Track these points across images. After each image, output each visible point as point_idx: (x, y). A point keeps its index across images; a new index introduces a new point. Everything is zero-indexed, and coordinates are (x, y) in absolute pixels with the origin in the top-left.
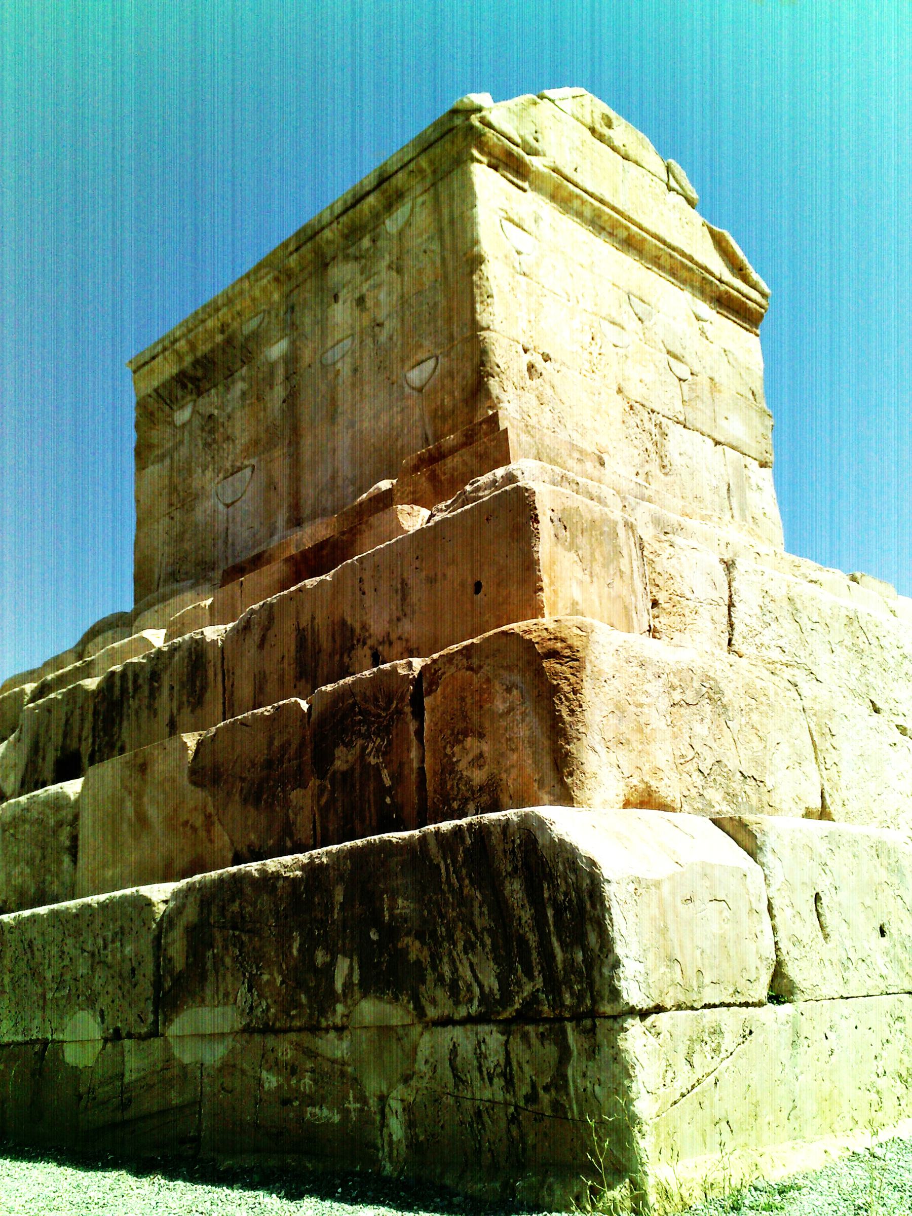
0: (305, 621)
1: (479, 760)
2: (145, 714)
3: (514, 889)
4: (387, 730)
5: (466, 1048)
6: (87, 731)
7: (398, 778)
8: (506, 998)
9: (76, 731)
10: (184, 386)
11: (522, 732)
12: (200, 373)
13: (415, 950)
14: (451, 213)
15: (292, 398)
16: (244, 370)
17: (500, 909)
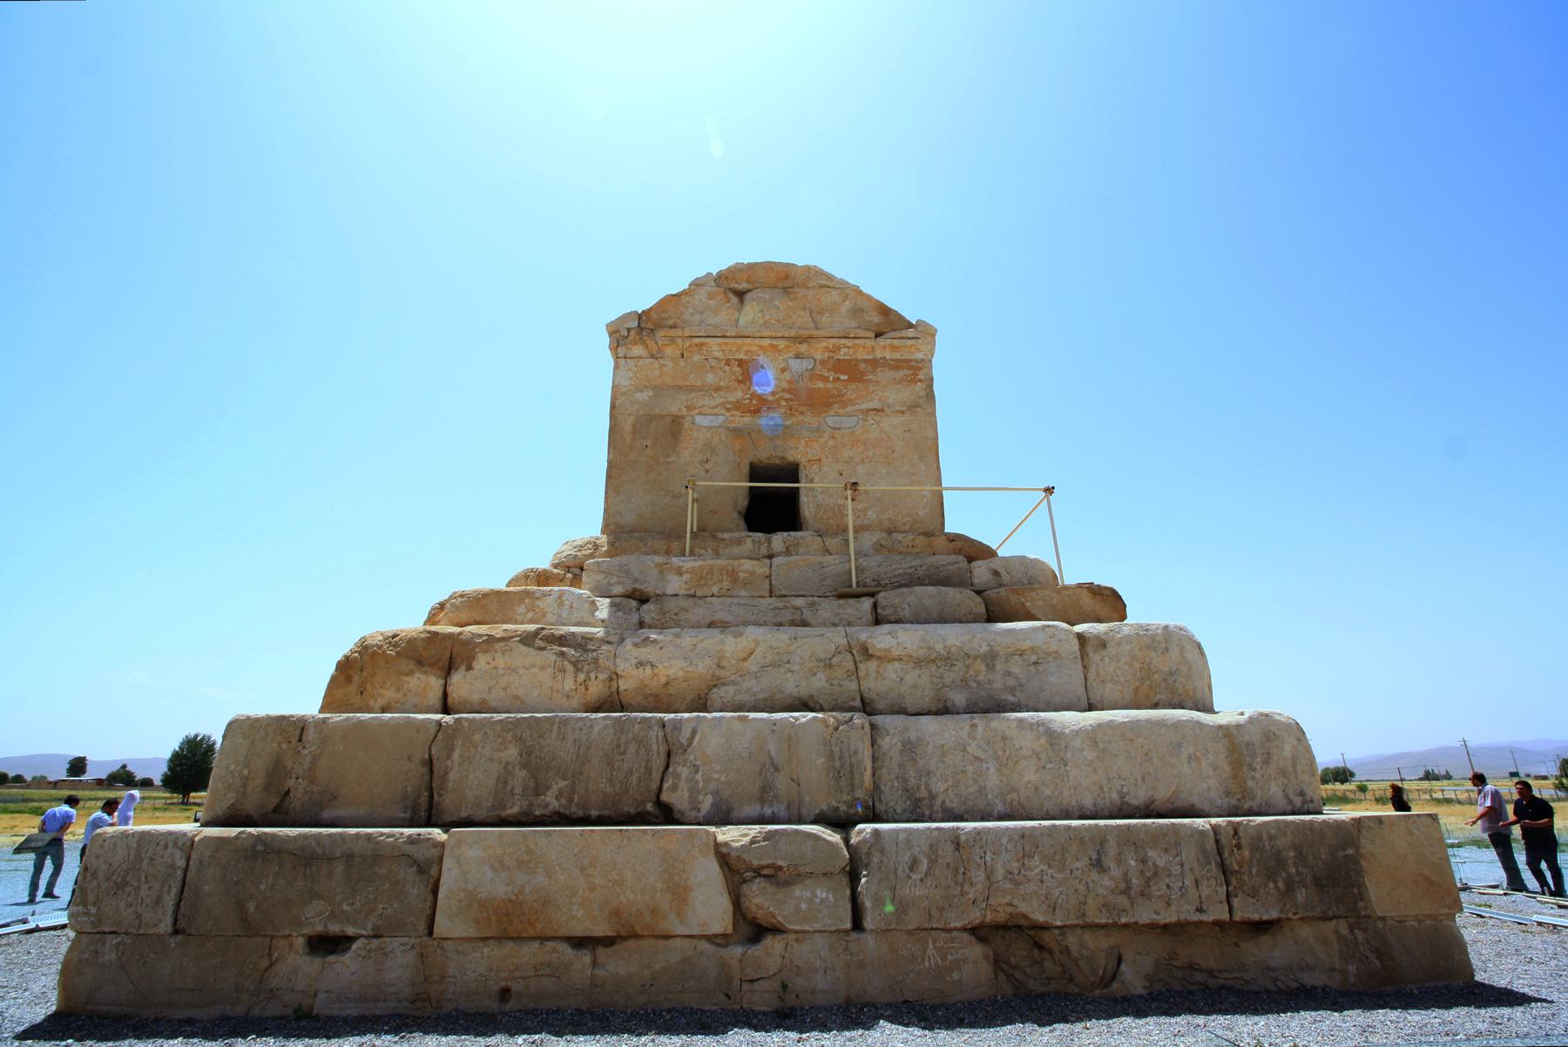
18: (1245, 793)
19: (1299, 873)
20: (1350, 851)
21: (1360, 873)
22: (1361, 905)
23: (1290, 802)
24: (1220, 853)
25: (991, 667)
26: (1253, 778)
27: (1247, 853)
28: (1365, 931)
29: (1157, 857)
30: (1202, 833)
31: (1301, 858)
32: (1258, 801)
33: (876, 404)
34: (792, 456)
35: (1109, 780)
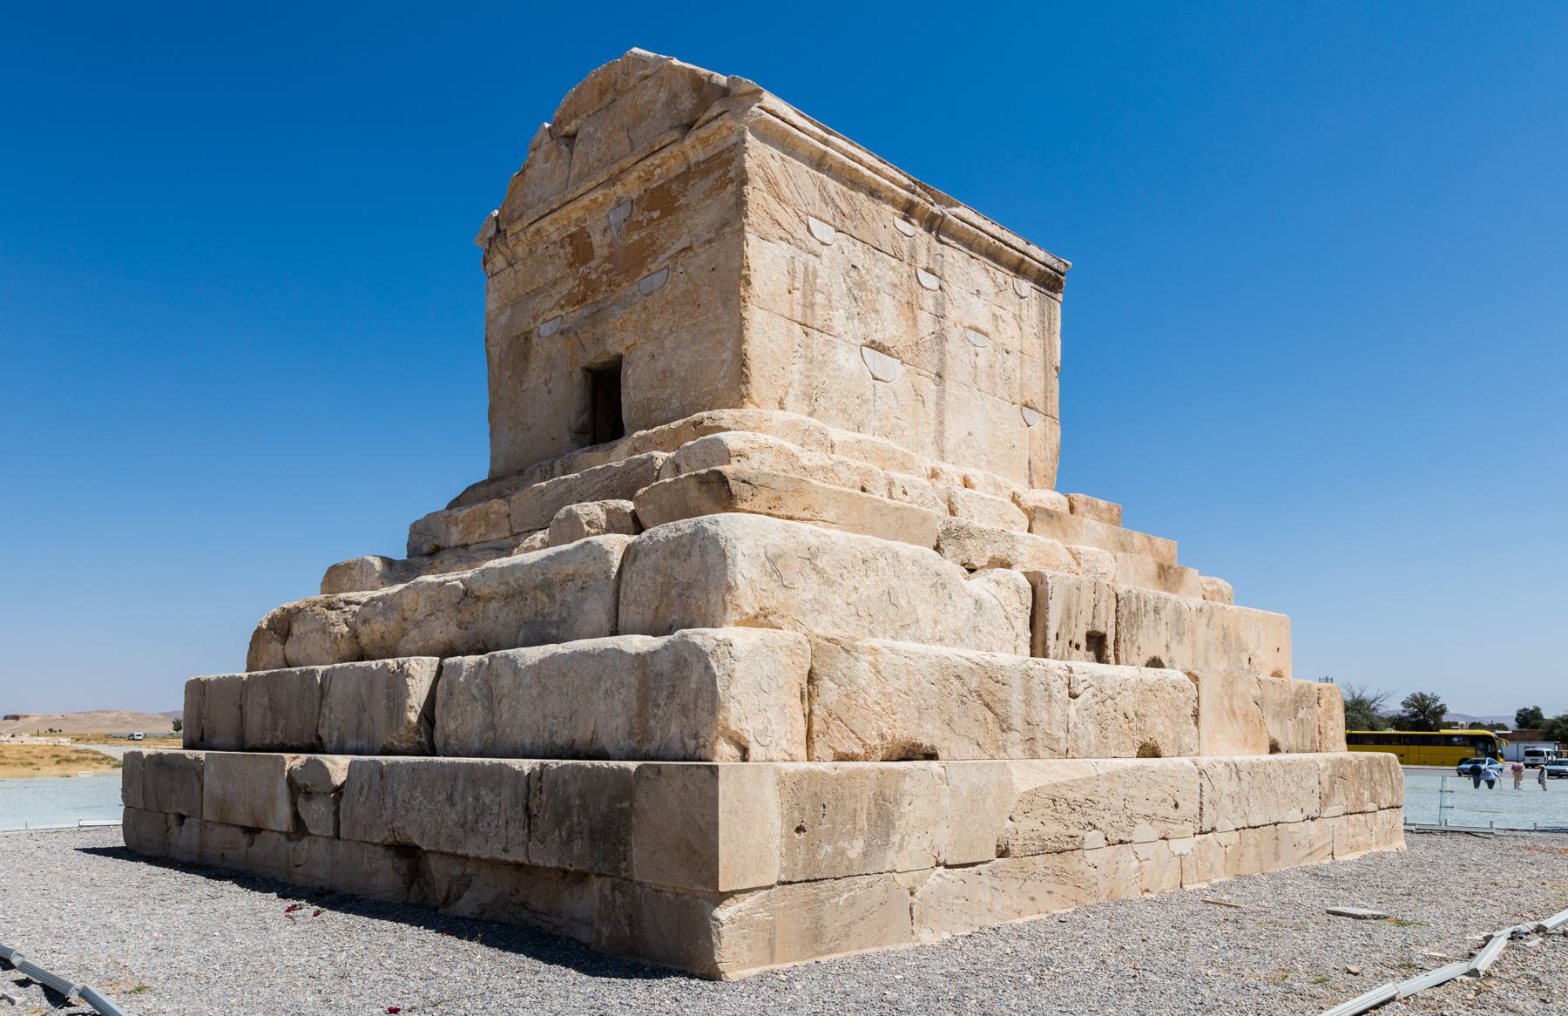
2: (1152, 632)
6: (1112, 621)
18: (646, 734)
19: (580, 823)
20: (626, 804)
21: (629, 830)
22: (623, 865)
23: (684, 745)
24: (527, 797)
25: (552, 597)
26: (655, 716)
27: (544, 797)
28: (624, 893)
29: (487, 797)
30: (519, 774)
31: (584, 807)
32: (655, 744)
33: (684, 243)
34: (614, 347)
35: (545, 718)
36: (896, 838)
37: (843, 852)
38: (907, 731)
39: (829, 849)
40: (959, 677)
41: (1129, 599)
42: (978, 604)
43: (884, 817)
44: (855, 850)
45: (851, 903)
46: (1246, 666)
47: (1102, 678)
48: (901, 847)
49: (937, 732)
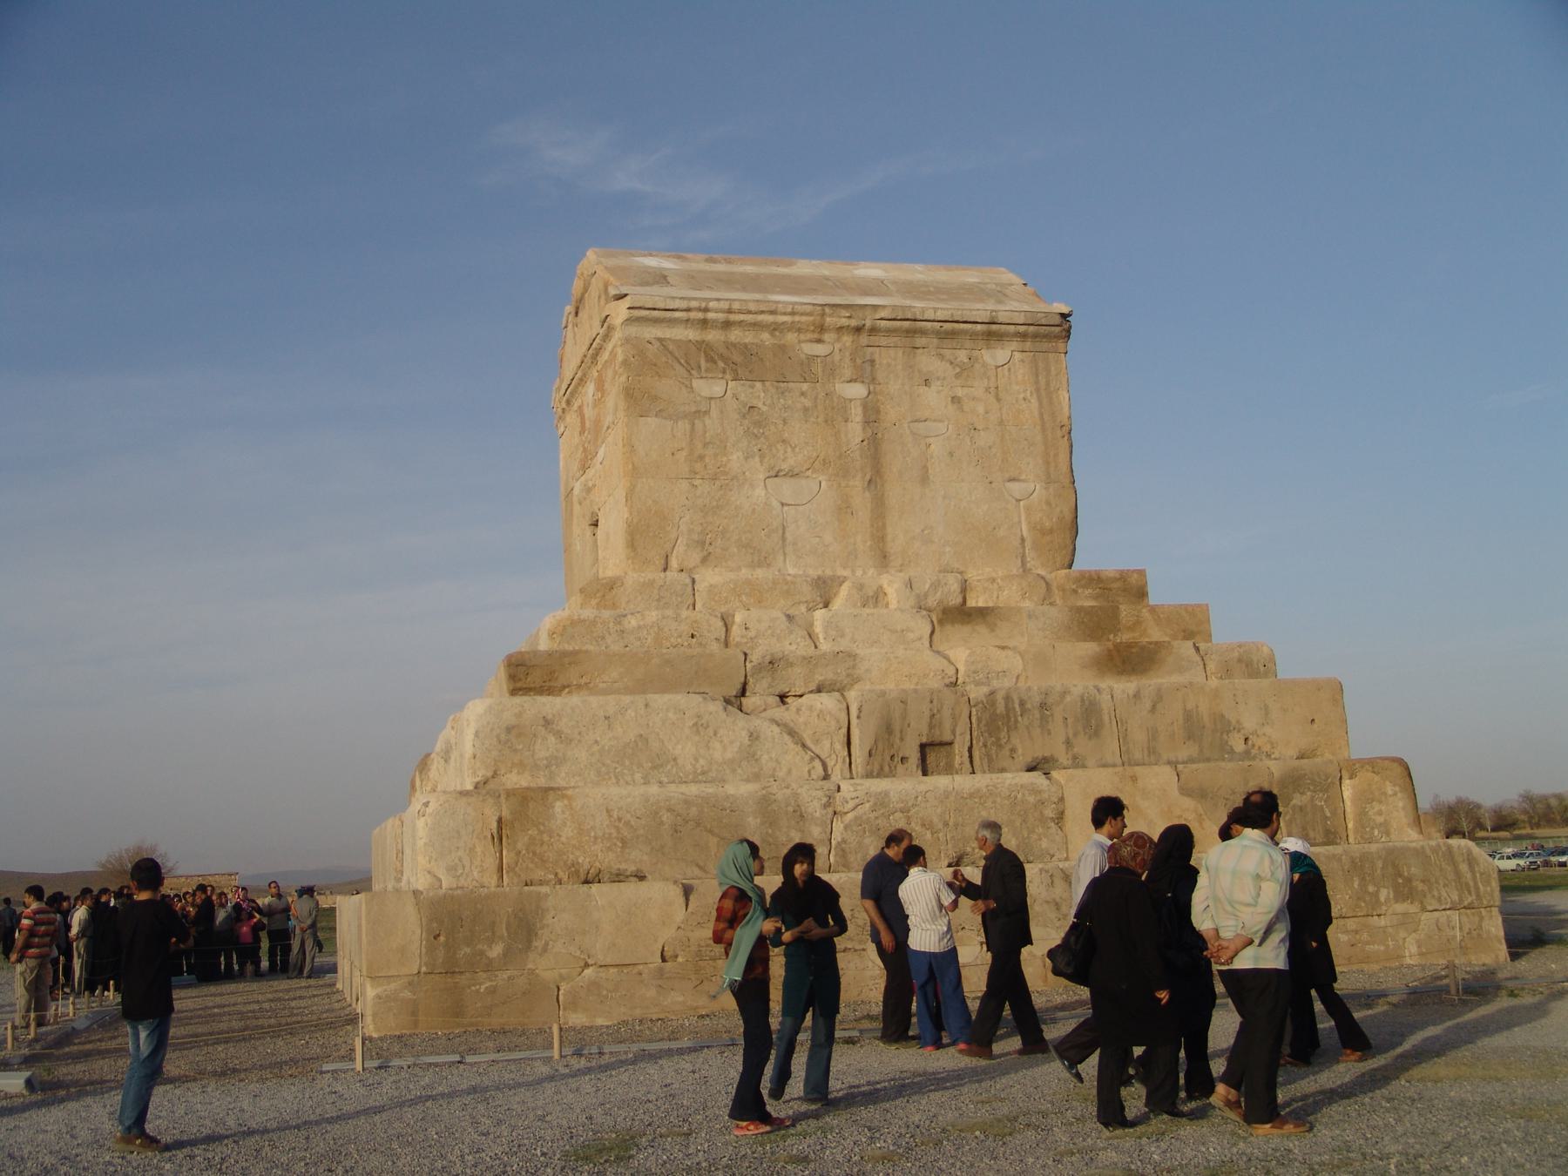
0: (1189, 707)
1: (1380, 813)
2: (1037, 732)
3: (1464, 867)
4: (1326, 791)
5: (1443, 920)
6: (963, 726)
7: (1334, 813)
8: (1461, 900)
9: (947, 725)
10: (710, 359)
11: (1401, 804)
12: (737, 358)
13: (1420, 886)
14: (1048, 384)
15: (874, 445)
16: (805, 386)
17: (1458, 873)
36: (538, 944)
37: (482, 953)
38: (608, 860)
39: (468, 950)
40: (669, 810)
41: (993, 704)
42: (754, 736)
43: (525, 929)
44: (496, 951)
45: (492, 991)
46: (1239, 746)
47: (887, 794)
48: (545, 950)
49: (645, 858)
